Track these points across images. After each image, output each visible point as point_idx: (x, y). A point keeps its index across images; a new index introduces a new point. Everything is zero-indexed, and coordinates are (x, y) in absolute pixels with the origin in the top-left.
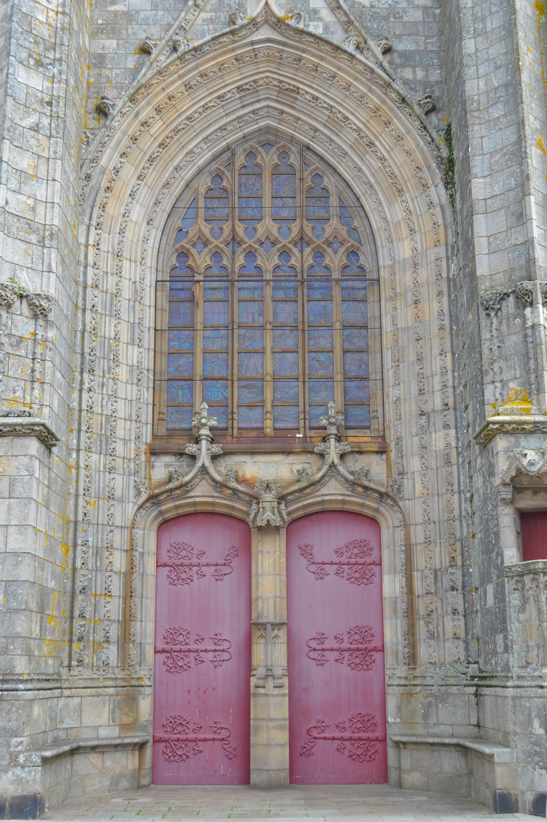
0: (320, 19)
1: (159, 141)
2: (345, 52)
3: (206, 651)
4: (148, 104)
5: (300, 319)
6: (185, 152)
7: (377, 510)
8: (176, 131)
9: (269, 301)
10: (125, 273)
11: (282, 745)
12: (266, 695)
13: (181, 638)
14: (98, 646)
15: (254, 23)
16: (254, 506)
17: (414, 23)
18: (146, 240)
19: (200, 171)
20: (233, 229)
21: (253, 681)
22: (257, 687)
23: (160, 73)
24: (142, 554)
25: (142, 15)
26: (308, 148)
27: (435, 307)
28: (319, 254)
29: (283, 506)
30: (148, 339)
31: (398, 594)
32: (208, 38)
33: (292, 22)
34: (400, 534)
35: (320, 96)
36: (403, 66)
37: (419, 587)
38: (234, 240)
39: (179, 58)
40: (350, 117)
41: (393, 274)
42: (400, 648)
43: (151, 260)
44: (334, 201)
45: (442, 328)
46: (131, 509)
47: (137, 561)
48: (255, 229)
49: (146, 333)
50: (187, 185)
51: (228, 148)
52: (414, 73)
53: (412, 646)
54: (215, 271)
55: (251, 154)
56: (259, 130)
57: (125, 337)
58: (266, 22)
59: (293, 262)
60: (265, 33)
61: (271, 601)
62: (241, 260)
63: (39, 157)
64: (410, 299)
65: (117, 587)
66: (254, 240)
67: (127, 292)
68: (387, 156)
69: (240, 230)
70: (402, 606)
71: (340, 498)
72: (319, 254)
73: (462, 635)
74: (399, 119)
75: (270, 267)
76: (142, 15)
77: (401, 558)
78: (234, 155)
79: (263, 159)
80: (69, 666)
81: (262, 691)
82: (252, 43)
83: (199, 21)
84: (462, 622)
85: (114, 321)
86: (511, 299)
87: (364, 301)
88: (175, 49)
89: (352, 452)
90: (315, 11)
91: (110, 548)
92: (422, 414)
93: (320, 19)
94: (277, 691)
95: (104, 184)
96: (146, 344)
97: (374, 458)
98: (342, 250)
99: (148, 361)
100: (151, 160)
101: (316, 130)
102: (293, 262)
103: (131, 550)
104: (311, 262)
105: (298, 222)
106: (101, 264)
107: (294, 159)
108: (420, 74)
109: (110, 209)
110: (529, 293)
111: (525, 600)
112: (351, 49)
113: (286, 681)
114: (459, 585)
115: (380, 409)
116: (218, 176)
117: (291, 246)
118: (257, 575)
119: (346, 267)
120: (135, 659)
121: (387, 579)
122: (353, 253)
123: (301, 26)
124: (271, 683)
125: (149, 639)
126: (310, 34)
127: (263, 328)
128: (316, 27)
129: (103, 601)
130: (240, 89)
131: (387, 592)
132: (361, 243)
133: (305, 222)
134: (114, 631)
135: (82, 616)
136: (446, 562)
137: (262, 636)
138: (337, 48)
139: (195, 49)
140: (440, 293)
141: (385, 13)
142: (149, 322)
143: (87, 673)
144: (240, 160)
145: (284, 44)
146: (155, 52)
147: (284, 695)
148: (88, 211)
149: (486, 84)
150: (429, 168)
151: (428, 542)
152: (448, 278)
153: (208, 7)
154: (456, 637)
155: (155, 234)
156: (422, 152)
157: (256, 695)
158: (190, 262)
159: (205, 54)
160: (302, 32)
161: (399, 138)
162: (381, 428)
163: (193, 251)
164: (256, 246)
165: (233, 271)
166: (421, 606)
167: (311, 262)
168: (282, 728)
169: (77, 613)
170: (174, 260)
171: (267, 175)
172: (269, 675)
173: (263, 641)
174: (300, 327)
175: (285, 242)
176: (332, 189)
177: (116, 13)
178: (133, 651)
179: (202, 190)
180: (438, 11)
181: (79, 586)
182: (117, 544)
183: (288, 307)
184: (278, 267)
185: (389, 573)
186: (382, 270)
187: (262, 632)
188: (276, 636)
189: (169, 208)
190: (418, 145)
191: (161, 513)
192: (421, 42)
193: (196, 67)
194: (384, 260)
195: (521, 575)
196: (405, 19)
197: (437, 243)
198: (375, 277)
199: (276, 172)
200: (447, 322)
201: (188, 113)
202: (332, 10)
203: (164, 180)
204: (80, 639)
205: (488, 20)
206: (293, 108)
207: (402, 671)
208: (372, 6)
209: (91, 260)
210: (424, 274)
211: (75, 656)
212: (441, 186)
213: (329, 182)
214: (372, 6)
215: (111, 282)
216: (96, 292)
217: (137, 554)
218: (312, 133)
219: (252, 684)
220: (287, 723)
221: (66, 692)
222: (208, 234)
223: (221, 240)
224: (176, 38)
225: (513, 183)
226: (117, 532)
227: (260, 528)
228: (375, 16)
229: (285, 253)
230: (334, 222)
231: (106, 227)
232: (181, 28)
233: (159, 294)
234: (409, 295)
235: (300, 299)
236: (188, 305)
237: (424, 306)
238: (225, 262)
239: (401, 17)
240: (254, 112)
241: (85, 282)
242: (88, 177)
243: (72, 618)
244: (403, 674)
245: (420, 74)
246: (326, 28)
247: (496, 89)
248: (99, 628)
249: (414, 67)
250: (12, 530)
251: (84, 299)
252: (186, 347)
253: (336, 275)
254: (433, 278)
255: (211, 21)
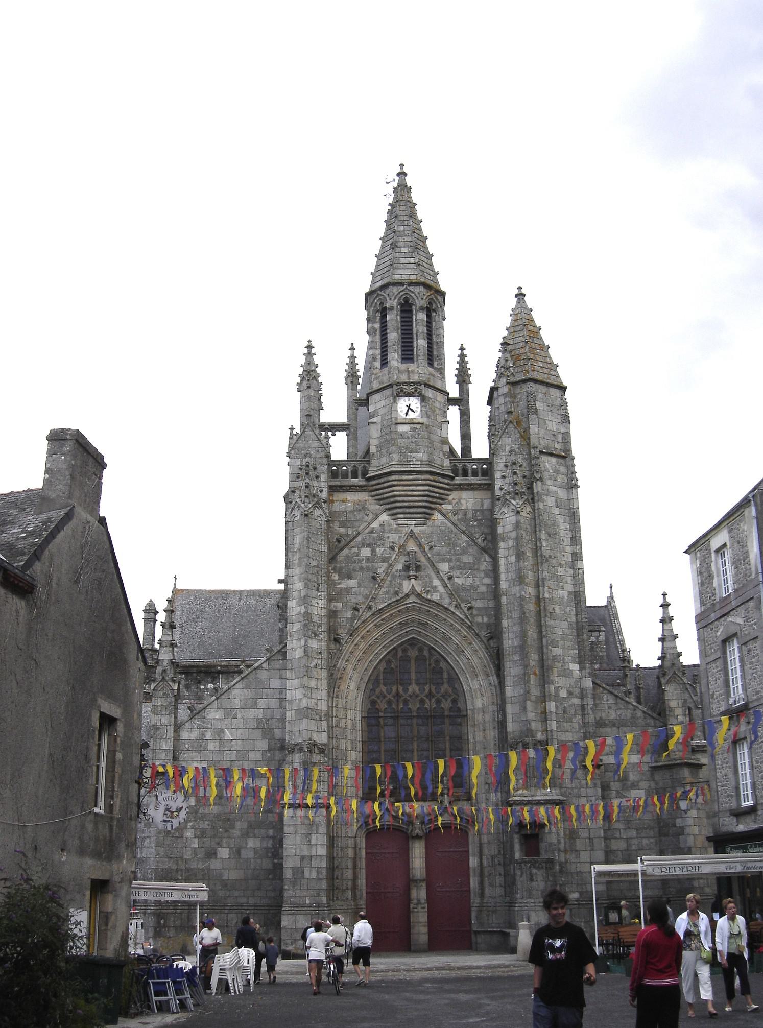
0: (438, 591)
1: (363, 651)
2: (450, 611)
3: (389, 892)
4: (358, 635)
5: (430, 734)
6: (374, 654)
7: (466, 827)
8: (370, 645)
9: (415, 725)
10: (349, 717)
11: (425, 934)
12: (418, 912)
13: (378, 887)
14: (343, 891)
15: (407, 595)
16: (410, 827)
17: (483, 593)
18: (357, 698)
19: (381, 660)
20: (397, 690)
21: (412, 906)
22: (413, 908)
23: (363, 622)
24: (360, 848)
25: (354, 590)
26: (432, 648)
27: (492, 734)
28: (438, 702)
29: (424, 826)
30: (359, 746)
31: (476, 865)
32: (386, 604)
33: (424, 595)
34: (477, 839)
35: (439, 627)
36: (478, 615)
37: (485, 863)
38: (398, 695)
39: (372, 614)
40: (453, 638)
41: (474, 714)
42: (477, 890)
43: (359, 708)
44: (445, 675)
45: (495, 744)
46: (355, 827)
47: (358, 852)
48: (408, 689)
49: (358, 744)
50: (375, 668)
51: (394, 648)
52: (483, 619)
53: (482, 888)
54: (389, 710)
55: (404, 651)
56: (409, 639)
57: (349, 748)
58: (413, 593)
59: (426, 706)
60: (412, 599)
61: (419, 870)
62: (401, 706)
63: (318, 679)
64: (481, 728)
65: (350, 865)
66: (407, 695)
67: (349, 727)
68: (470, 658)
69: (401, 689)
70: (478, 871)
71: (449, 822)
72: (438, 702)
73: (503, 885)
74: (476, 642)
75: (415, 709)
76: (354, 590)
77: (477, 850)
78: (397, 651)
79: (411, 653)
80: (333, 900)
81: (416, 910)
82: (406, 604)
83: (381, 593)
84: (503, 879)
85: (345, 741)
86: (521, 744)
87: (460, 724)
88: (370, 608)
89: (455, 800)
90: (436, 587)
91: (347, 847)
92: (487, 784)
93: (438, 591)
94: (422, 910)
95: (339, 676)
96: (358, 749)
97: (465, 802)
98: (449, 700)
99: (359, 758)
100: (359, 661)
101: (436, 641)
102: (426, 706)
103: (355, 848)
104: (435, 706)
105: (428, 686)
106: (339, 715)
107: (426, 653)
108: (485, 620)
109: (341, 687)
110: (527, 744)
111: (522, 874)
112: (452, 609)
113: (426, 905)
114: (502, 863)
115: (468, 779)
116: (389, 662)
117: (425, 698)
118: (412, 858)
119: (451, 708)
120: (358, 897)
121: (471, 859)
122: (454, 701)
123: (429, 597)
124: (420, 906)
125: (364, 888)
126: (433, 601)
127: (412, 738)
128: (437, 595)
129: (345, 871)
130: (400, 623)
131: (471, 865)
132: (458, 695)
133: (432, 686)
134: (350, 884)
135: (337, 878)
136: (497, 852)
137: (415, 886)
138: (447, 609)
139: (380, 610)
140: (494, 728)
141: (468, 588)
142: (359, 738)
143: (340, 903)
144: (400, 653)
145: (421, 604)
146: (361, 611)
147: (426, 911)
148: (332, 691)
149: (512, 643)
150: (489, 666)
151: (489, 843)
152: (498, 721)
153: (385, 586)
154: (501, 886)
155: (361, 694)
156: (486, 659)
157: (413, 912)
158: (377, 707)
159: (385, 610)
160: (429, 600)
161: (476, 651)
162: (468, 788)
163: (379, 701)
164: (409, 698)
165: (398, 711)
166: (486, 871)
167: (435, 706)
168: (424, 926)
169: (335, 877)
170: (369, 705)
171: (413, 662)
172: (419, 902)
173: (416, 888)
174: (430, 739)
175: (422, 696)
176: (444, 668)
177: (341, 589)
178: (358, 893)
179: (382, 670)
180: (494, 587)
181: (335, 865)
182: (350, 846)
183: (424, 728)
184: (418, 708)
185: (472, 856)
186: (469, 711)
187: (415, 884)
188: (422, 886)
189: (366, 681)
190: (484, 655)
191: (368, 829)
192: (486, 603)
193: (380, 616)
194: (470, 707)
195: (521, 863)
196: (479, 591)
197: (493, 703)
198: (465, 714)
199: (417, 659)
200: (497, 742)
201: (376, 637)
202: (444, 587)
203: (364, 668)
204: (337, 888)
205: (513, 612)
206: (426, 631)
207: (478, 900)
208: (463, 584)
209: (334, 715)
210: (488, 717)
211: (335, 896)
212: (495, 677)
213: (443, 665)
214: (463, 584)
215: (342, 724)
216: (337, 729)
217: (357, 849)
218: (434, 642)
219: (411, 907)
220: (427, 924)
221: (333, 911)
222: (385, 693)
223: (391, 695)
224: (370, 604)
225: (522, 692)
226: (350, 839)
227: (413, 837)
228: (464, 590)
229: (422, 701)
230: (446, 686)
231: (340, 697)
232: (372, 598)
233: (363, 723)
234: (481, 726)
235: (430, 725)
236: (376, 727)
237: (487, 732)
238: (394, 706)
239: (476, 590)
240: (406, 632)
241: (332, 724)
242: (332, 675)
243: (333, 879)
244: (478, 902)
245: (485, 620)
246: (441, 596)
247: (516, 647)
248: (344, 883)
249: (482, 616)
250: (318, 846)
251: (333, 733)
252: (376, 748)
253: (446, 713)
254: (491, 720)
255: (387, 593)
